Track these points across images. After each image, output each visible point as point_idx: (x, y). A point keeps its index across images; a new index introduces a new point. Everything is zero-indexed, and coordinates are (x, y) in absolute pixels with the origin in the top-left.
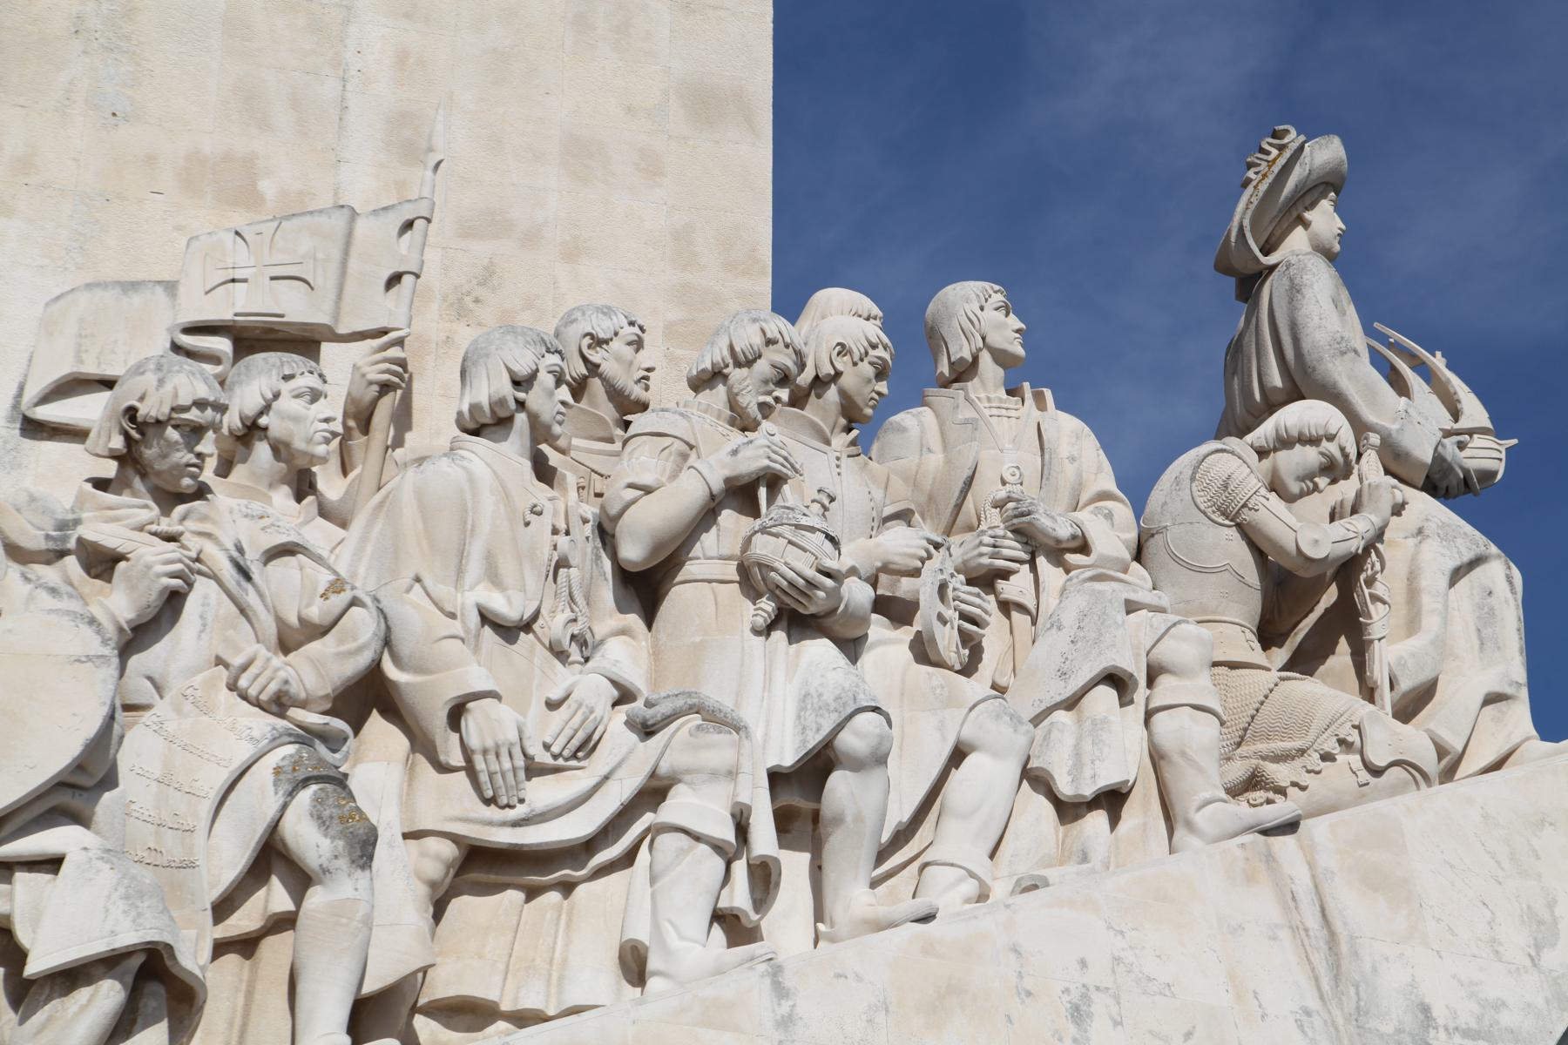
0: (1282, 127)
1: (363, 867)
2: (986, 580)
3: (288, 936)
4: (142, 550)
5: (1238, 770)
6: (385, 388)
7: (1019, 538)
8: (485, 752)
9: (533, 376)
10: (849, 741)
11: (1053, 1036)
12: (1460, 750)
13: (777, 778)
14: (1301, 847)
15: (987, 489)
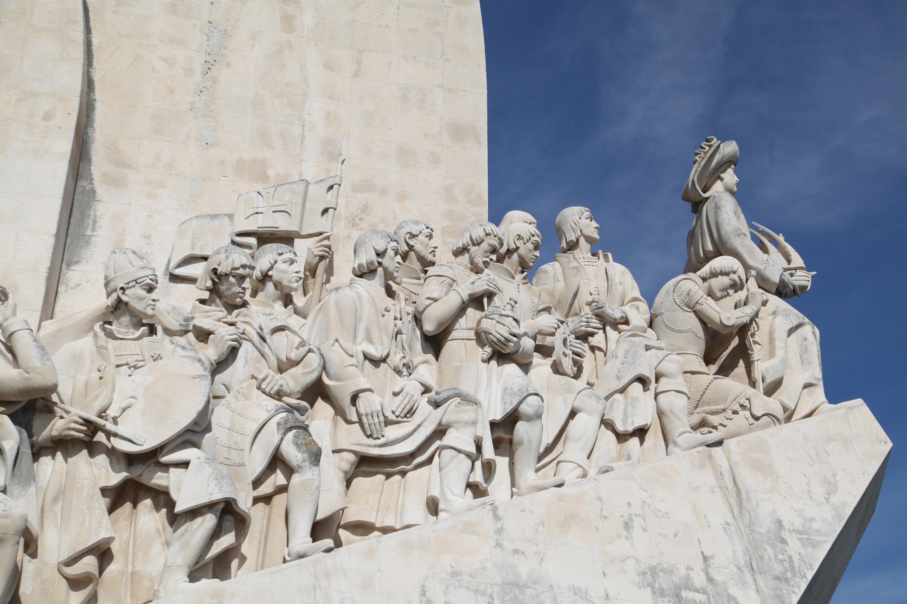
0: (710, 137)
1: (315, 465)
2: (584, 337)
3: (284, 495)
5: (696, 419)
6: (322, 258)
7: (598, 318)
8: (367, 415)
9: (385, 251)
10: (525, 408)
11: (616, 536)
12: (793, 408)
13: (493, 425)
14: (724, 452)
15: (584, 297)
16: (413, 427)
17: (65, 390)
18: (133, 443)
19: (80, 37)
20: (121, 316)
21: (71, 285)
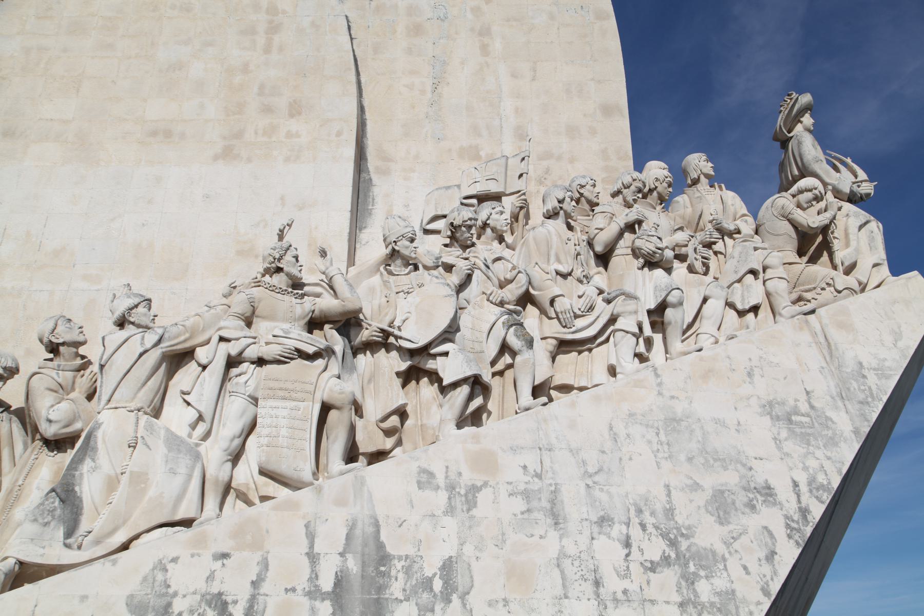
1: (530, 349)
2: (709, 245)
4: (459, 263)
5: (794, 296)
6: (521, 208)
8: (562, 312)
9: (564, 199)
10: (671, 299)
12: (866, 282)
13: (649, 312)
14: (817, 318)
15: (707, 217)
16: (594, 318)
17: (367, 311)
18: (412, 342)
19: (353, 78)
20: (395, 260)
21: (363, 242)
